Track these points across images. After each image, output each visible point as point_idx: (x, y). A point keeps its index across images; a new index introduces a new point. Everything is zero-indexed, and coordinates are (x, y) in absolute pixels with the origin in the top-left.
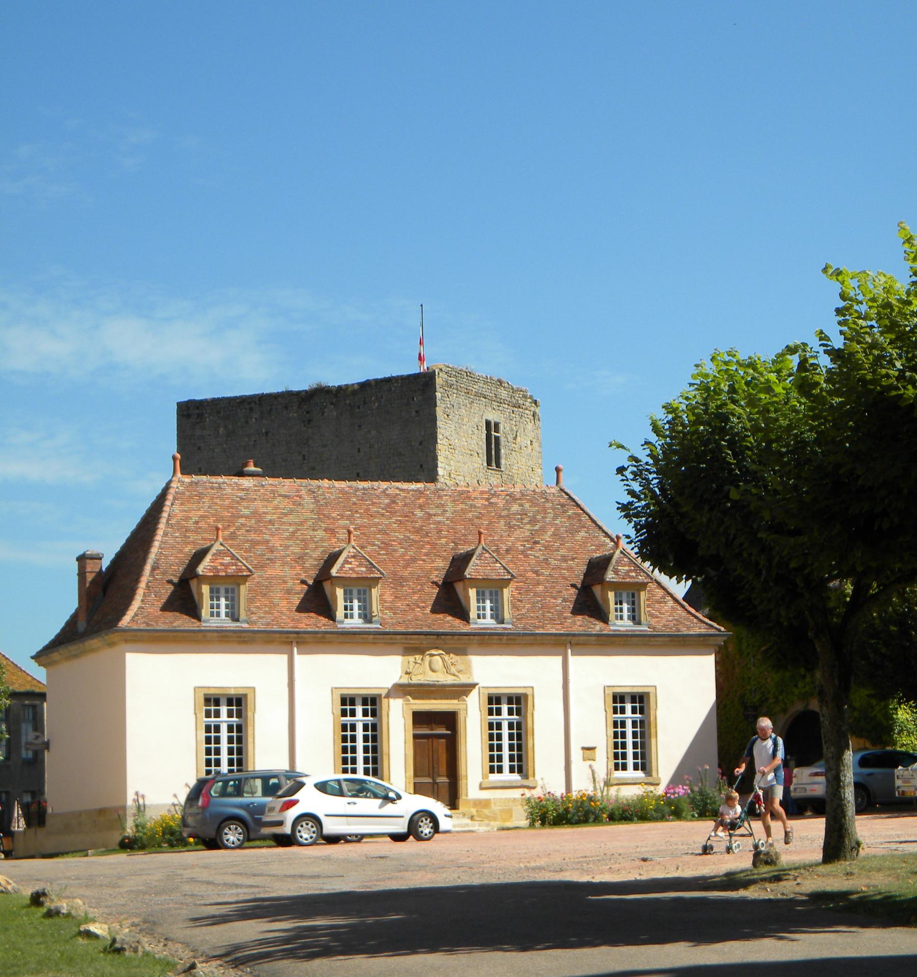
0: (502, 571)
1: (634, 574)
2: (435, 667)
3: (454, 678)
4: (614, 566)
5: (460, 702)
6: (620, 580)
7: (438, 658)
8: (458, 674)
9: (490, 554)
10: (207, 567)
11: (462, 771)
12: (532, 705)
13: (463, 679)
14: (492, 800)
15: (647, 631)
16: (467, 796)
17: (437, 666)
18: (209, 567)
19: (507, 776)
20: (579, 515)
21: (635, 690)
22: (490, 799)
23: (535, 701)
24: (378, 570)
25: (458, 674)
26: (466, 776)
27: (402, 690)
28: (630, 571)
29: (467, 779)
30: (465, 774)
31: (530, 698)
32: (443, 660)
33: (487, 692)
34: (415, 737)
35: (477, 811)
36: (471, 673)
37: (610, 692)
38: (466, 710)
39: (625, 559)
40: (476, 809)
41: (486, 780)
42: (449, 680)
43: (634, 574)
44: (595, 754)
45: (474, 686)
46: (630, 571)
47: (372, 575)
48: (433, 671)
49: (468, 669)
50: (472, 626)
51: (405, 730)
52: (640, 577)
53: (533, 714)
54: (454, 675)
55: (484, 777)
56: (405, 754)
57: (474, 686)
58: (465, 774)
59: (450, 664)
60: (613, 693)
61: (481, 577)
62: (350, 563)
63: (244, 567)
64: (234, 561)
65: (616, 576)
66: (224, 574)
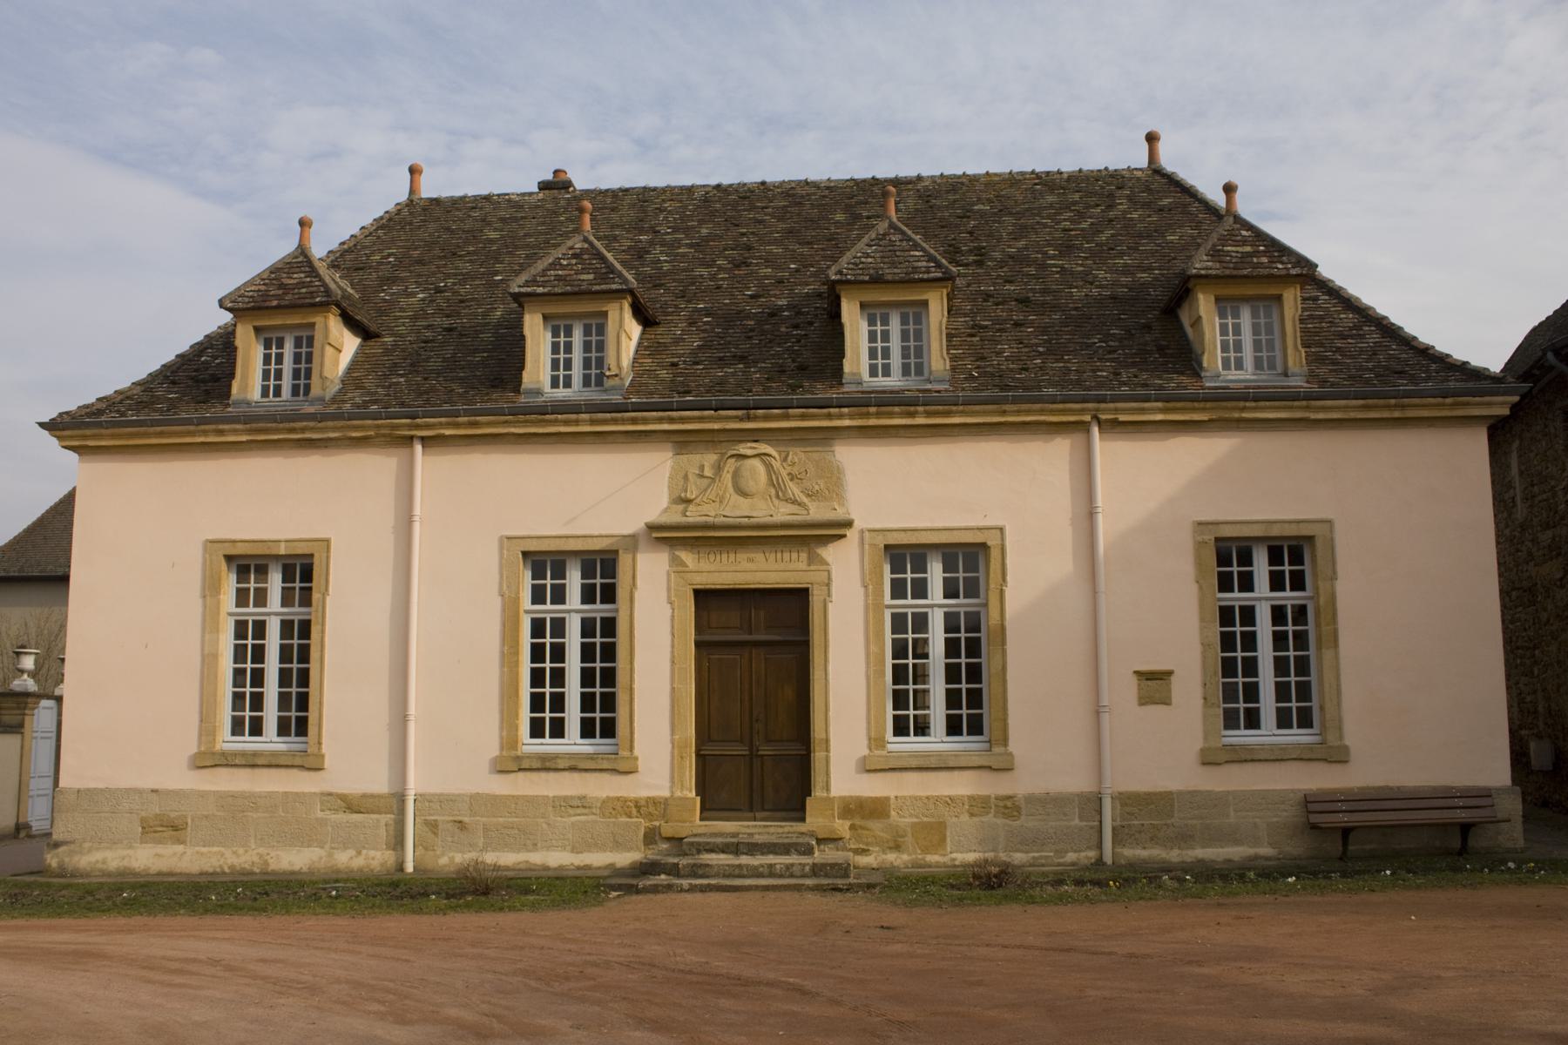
0: (924, 264)
1: (1265, 260)
2: (750, 486)
3: (795, 509)
4: (1214, 245)
5: (812, 568)
6: (1227, 272)
7: (756, 463)
8: (805, 500)
9: (903, 233)
10: (246, 294)
11: (817, 732)
12: (999, 572)
13: (817, 512)
14: (893, 801)
15: (1301, 387)
16: (828, 789)
17: (751, 483)
18: (251, 294)
19: (937, 742)
20: (1185, 206)
21: (1275, 531)
22: (887, 799)
23: (1008, 561)
24: (620, 275)
25: (805, 500)
26: (827, 741)
27: (664, 535)
28: (1256, 253)
29: (827, 750)
30: (824, 736)
31: (995, 554)
32: (769, 467)
33: (881, 541)
34: (699, 645)
35: (852, 827)
36: (841, 499)
37: (1209, 537)
38: (828, 585)
39: (1244, 233)
40: (848, 823)
41: (878, 752)
42: (783, 513)
43: (1265, 260)
44: (1169, 691)
45: (848, 524)
46: (1256, 253)
47: (604, 287)
48: (743, 493)
49: (834, 484)
50: (846, 389)
51: (673, 635)
52: (1280, 266)
53: (1002, 593)
54: (794, 502)
55: (876, 742)
56: (673, 689)
57: (848, 524)
58: (824, 736)
59: (787, 478)
60: (1217, 540)
61: (867, 278)
62: (563, 267)
63: (322, 289)
64: (308, 279)
65: (1218, 265)
66: (275, 303)
